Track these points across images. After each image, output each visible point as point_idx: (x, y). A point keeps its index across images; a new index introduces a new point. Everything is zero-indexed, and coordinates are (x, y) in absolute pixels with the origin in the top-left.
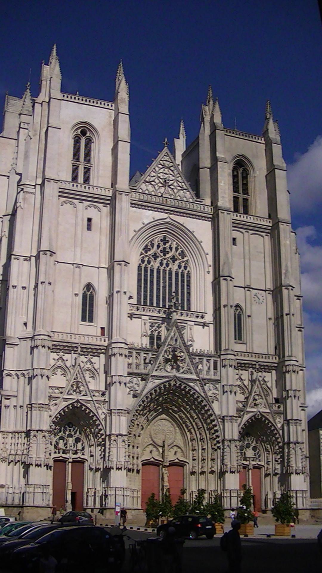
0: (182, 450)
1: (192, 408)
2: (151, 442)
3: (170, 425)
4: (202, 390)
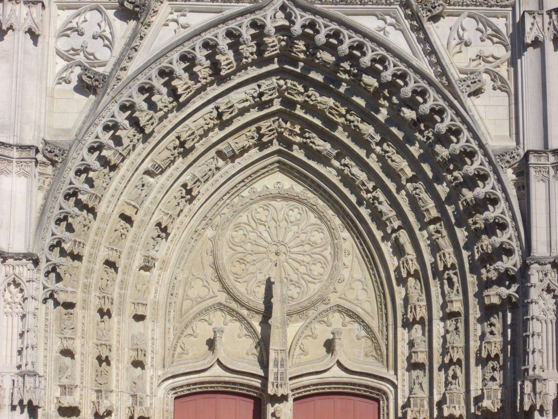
0: (367, 327)
1: (386, 136)
2: (222, 297)
3: (313, 218)
4: (419, 48)
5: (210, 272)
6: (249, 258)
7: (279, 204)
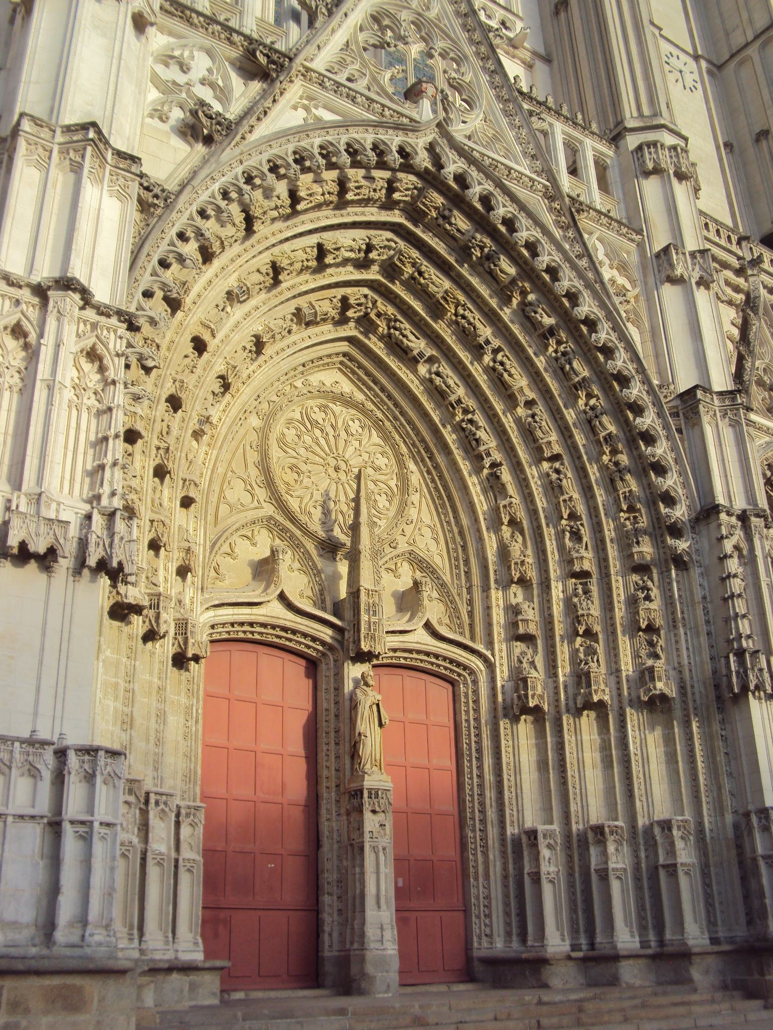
2: (269, 510)
3: (376, 438)
5: (254, 472)
6: (304, 467)
7: (337, 408)
